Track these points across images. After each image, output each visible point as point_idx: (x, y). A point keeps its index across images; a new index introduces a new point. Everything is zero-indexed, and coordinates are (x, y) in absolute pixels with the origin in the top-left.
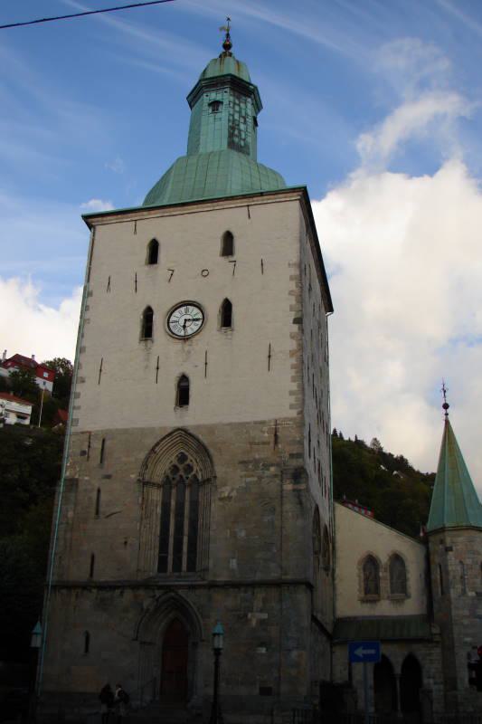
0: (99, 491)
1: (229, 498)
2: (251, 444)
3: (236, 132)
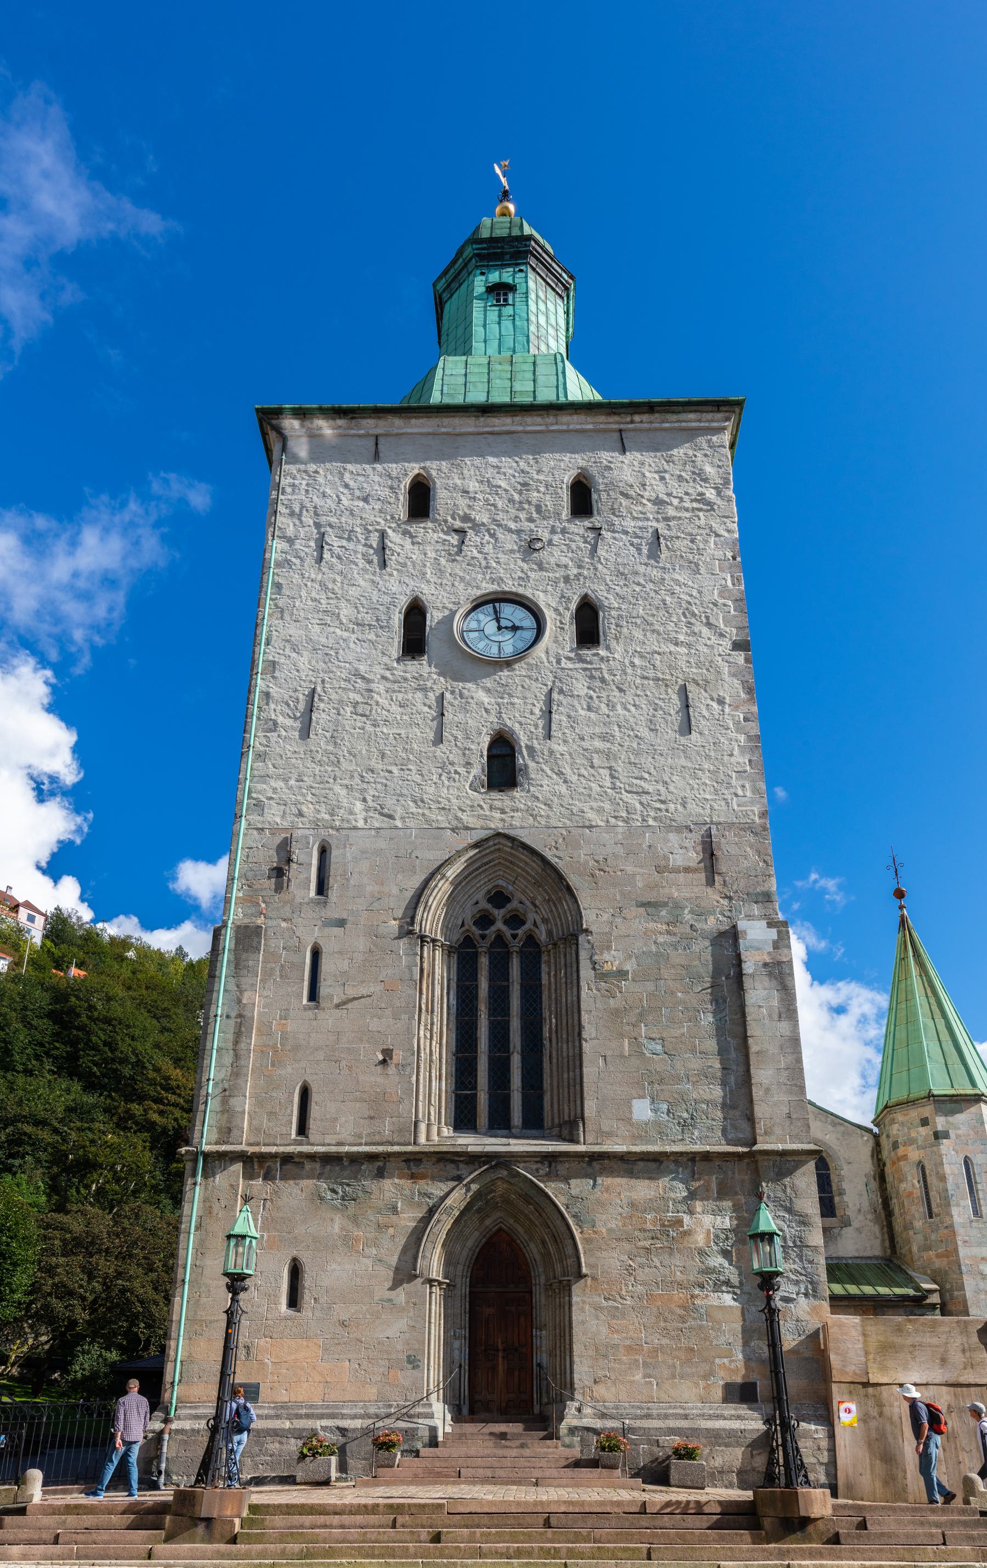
2: (659, 870)
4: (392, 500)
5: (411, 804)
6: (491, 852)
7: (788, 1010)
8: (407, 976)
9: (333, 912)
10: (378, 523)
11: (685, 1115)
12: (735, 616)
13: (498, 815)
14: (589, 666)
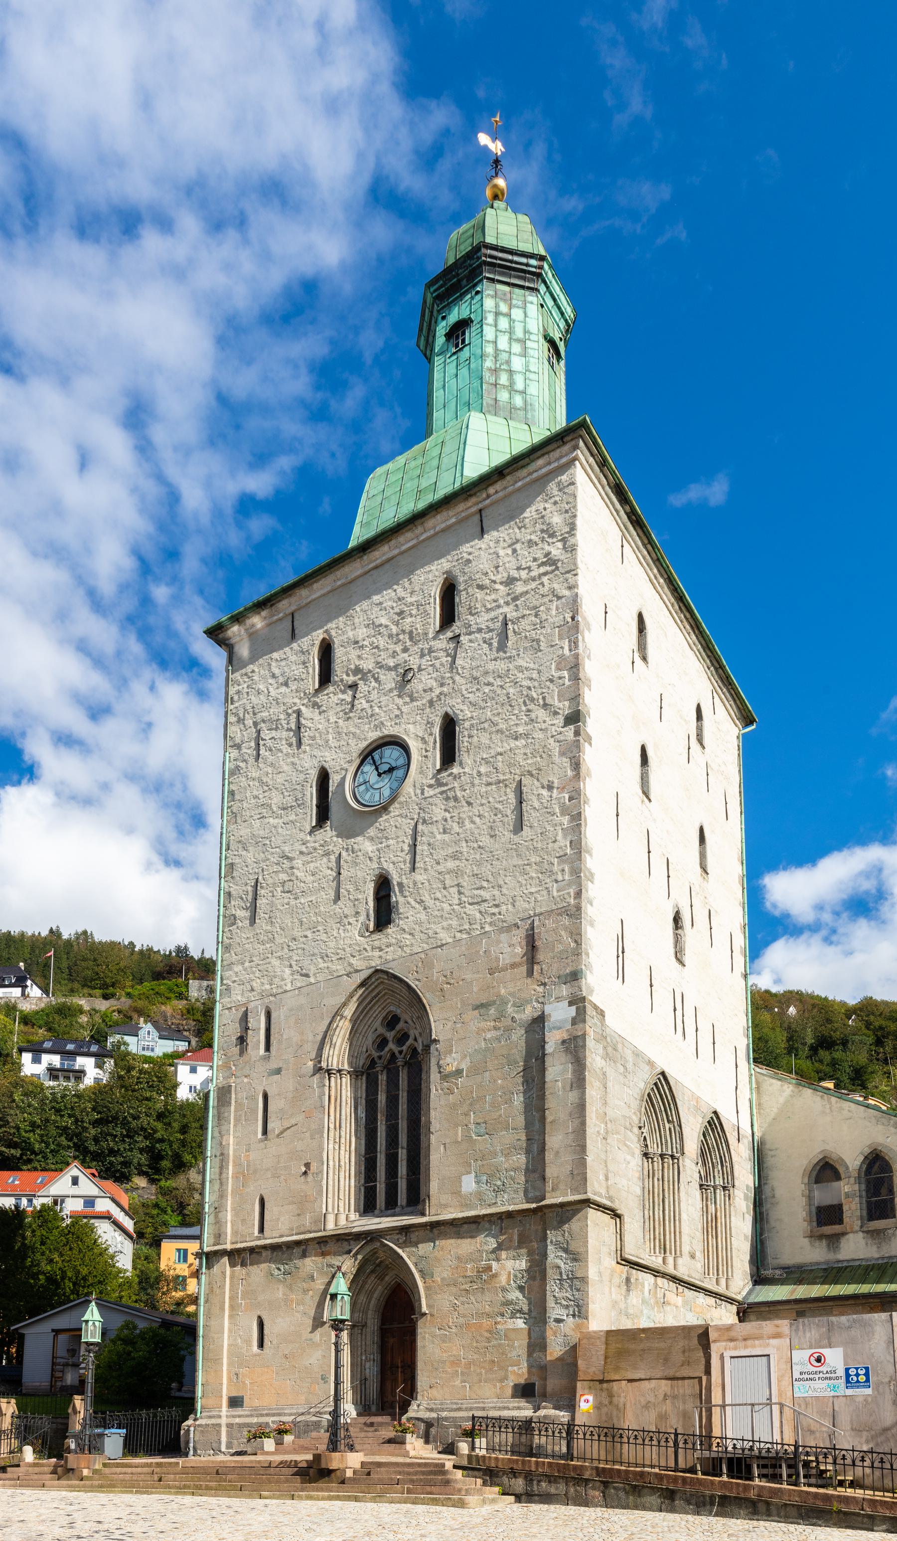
0: (266, 1097)
1: (459, 1072)
3: (504, 379)
4: (304, 676)
5: (320, 960)
6: (376, 987)
7: (579, 1079)
8: (319, 1104)
9: (274, 1064)
10: (295, 704)
11: (499, 1183)
12: (569, 687)
13: (377, 953)
14: (445, 788)
